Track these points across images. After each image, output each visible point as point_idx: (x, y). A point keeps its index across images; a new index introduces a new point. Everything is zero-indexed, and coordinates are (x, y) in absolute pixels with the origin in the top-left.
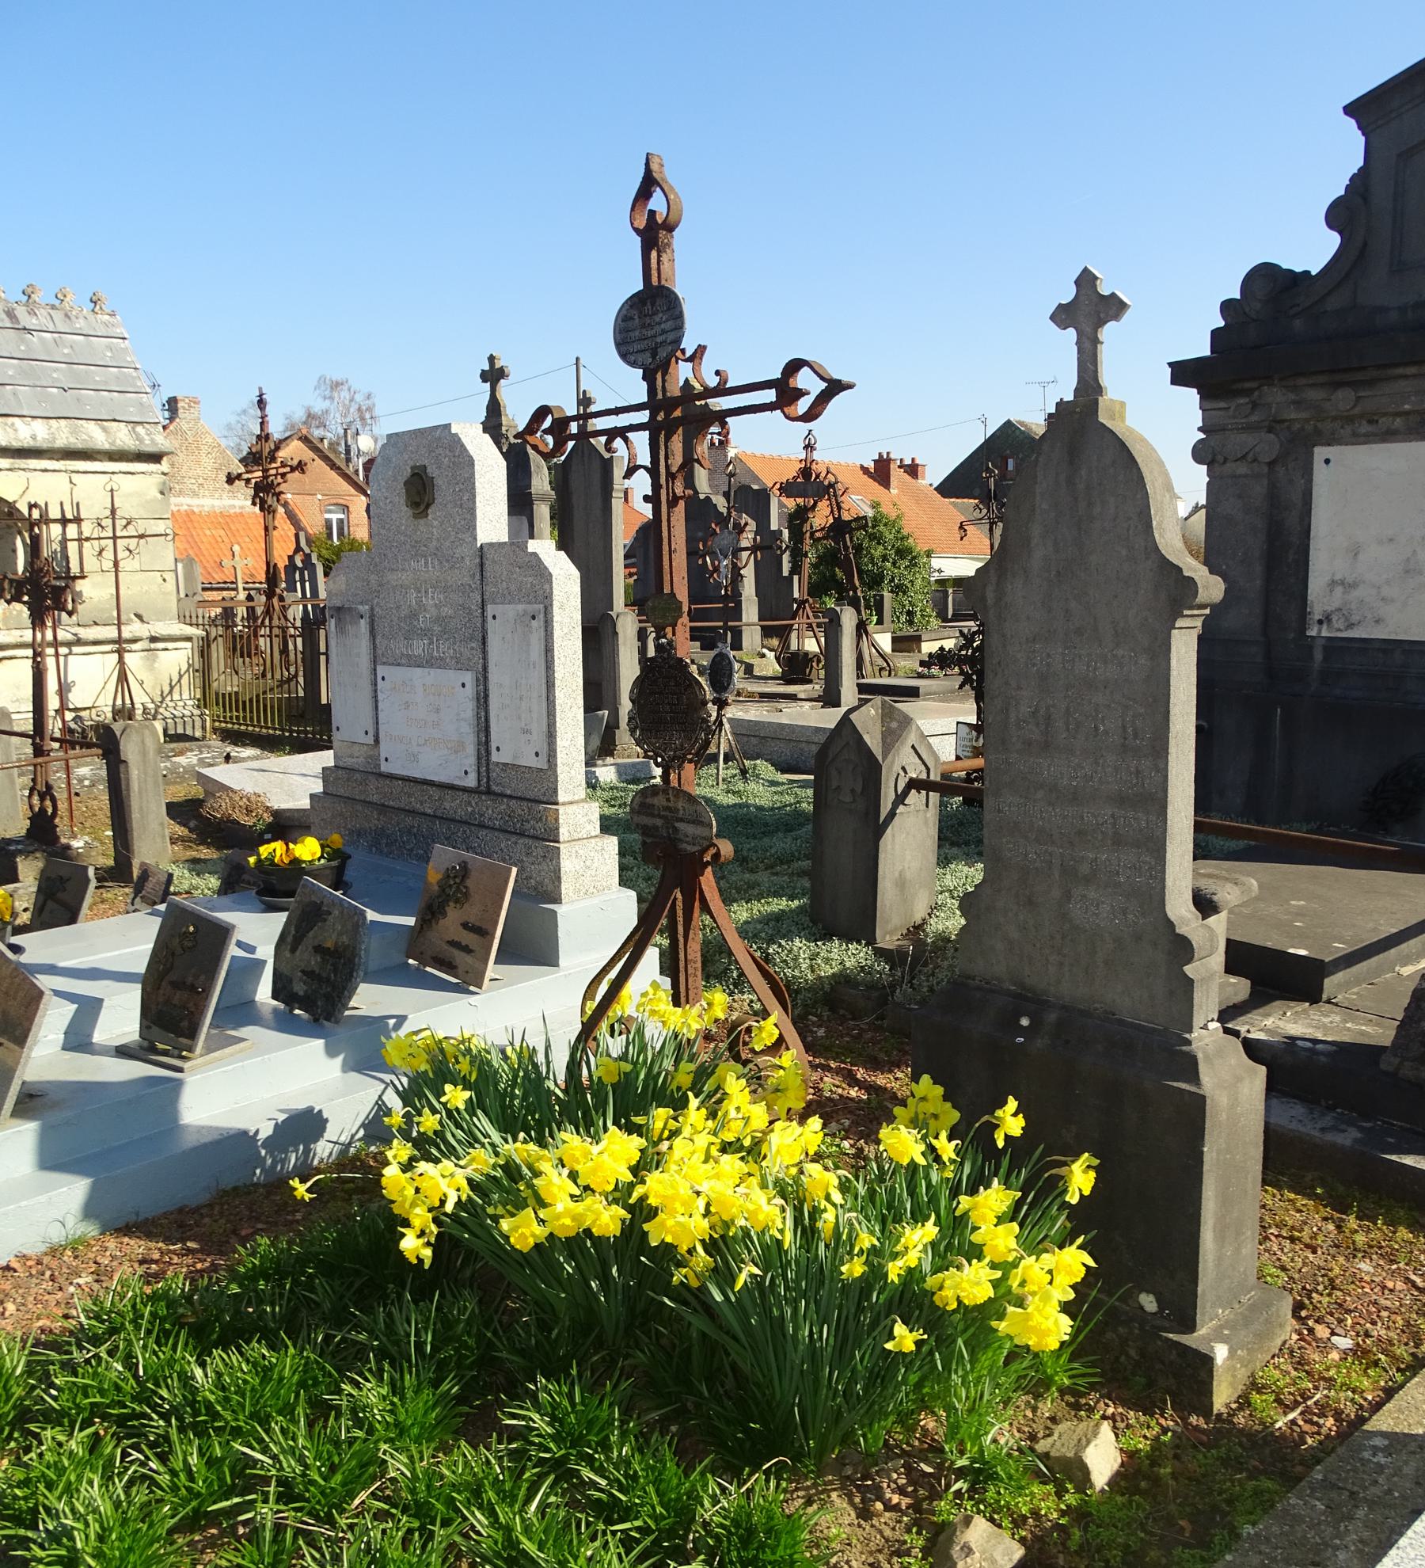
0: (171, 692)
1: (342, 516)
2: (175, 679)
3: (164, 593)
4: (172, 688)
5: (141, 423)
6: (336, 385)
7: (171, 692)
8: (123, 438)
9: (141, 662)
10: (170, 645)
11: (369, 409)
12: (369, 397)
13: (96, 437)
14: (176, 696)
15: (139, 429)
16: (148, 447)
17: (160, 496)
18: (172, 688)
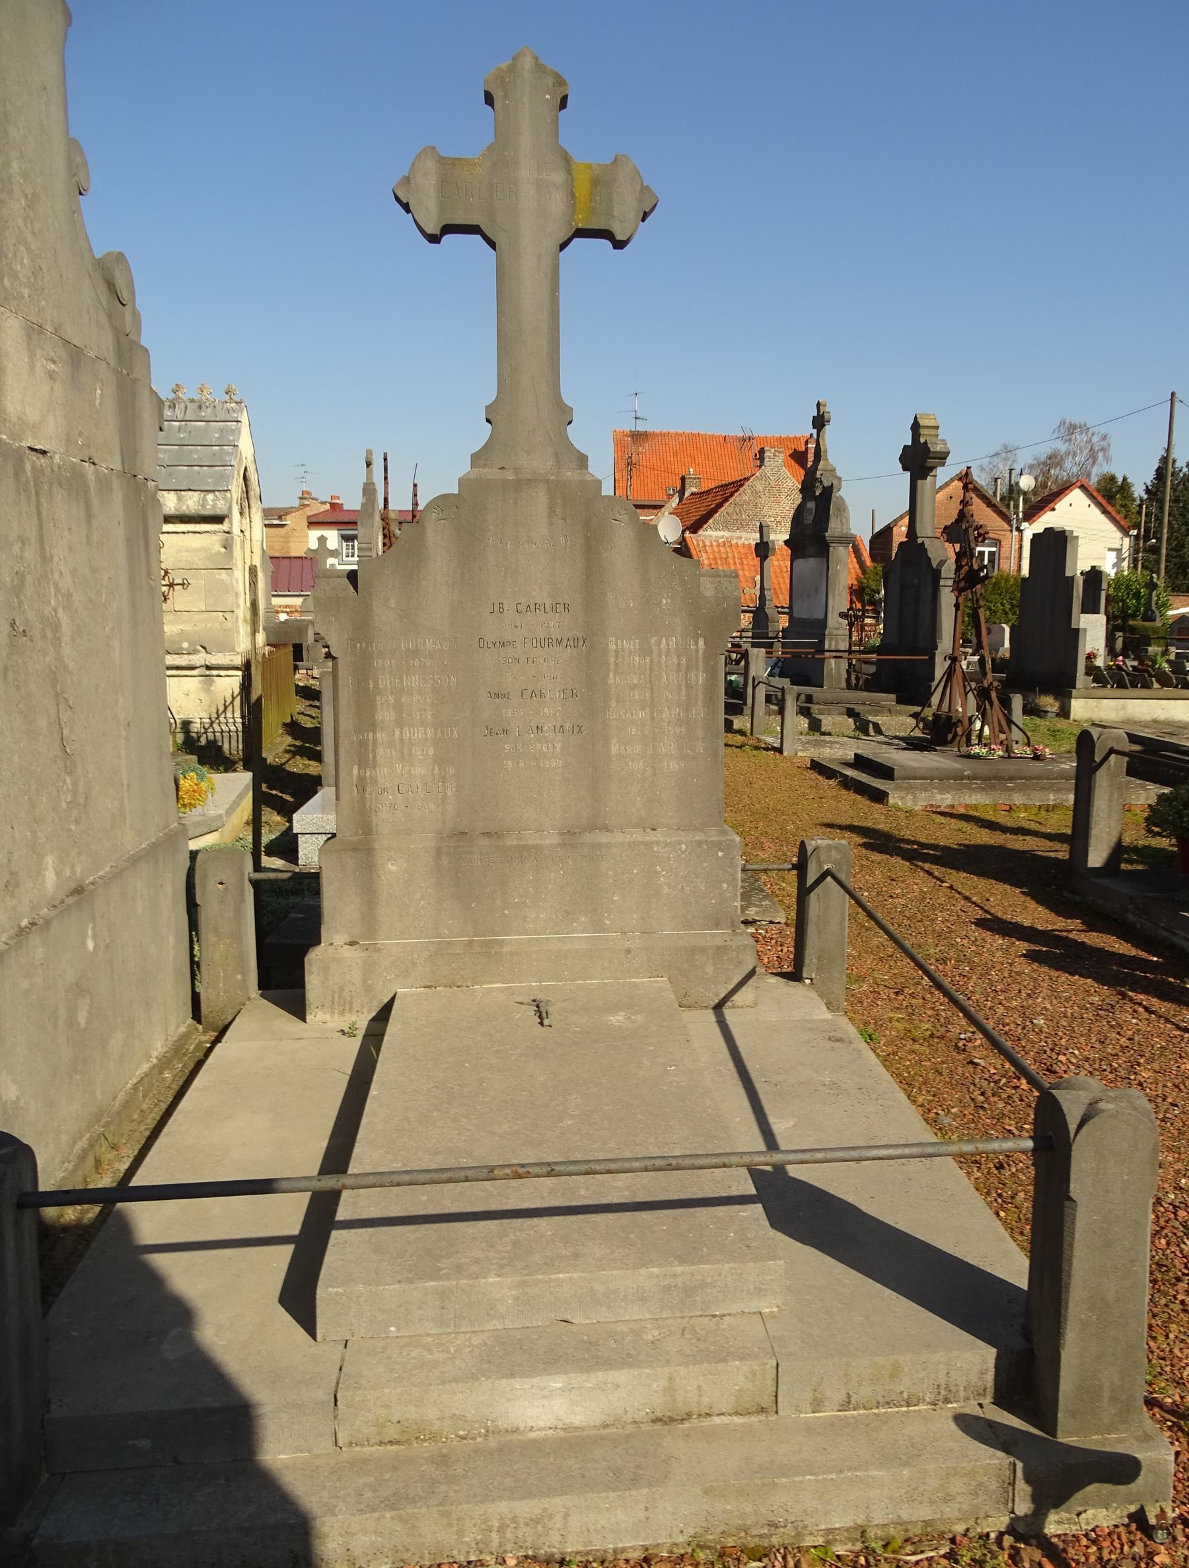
0: (225, 711)
1: (994, 549)
2: (229, 700)
4: (226, 708)
5: (213, 491)
6: (1072, 428)
7: (225, 711)
8: (192, 503)
9: (199, 686)
10: (222, 673)
11: (1103, 449)
12: (1105, 437)
14: (229, 715)
15: (210, 497)
16: (208, 511)
17: (223, 550)
18: (226, 708)
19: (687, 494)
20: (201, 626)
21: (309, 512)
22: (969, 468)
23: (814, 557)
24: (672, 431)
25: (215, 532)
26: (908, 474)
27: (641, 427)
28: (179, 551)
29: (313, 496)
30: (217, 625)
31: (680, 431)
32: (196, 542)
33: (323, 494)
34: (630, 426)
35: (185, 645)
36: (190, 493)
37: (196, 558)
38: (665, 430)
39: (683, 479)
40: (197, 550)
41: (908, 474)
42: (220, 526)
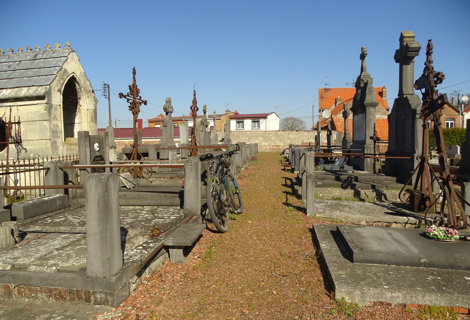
3: (47, 148)
8: (32, 92)
13: (24, 92)
15: (41, 88)
16: (37, 94)
19: (337, 104)
20: (37, 147)
21: (228, 115)
22: (430, 40)
23: (361, 113)
24: (337, 88)
25: (42, 104)
26: (399, 64)
27: (327, 87)
28: (28, 113)
29: (192, 104)
30: (44, 146)
31: (340, 87)
32: (34, 108)
33: (233, 110)
34: (324, 87)
35: (32, 155)
36: (34, 87)
38: (335, 88)
39: (336, 100)
40: (35, 112)
41: (399, 64)
42: (43, 101)
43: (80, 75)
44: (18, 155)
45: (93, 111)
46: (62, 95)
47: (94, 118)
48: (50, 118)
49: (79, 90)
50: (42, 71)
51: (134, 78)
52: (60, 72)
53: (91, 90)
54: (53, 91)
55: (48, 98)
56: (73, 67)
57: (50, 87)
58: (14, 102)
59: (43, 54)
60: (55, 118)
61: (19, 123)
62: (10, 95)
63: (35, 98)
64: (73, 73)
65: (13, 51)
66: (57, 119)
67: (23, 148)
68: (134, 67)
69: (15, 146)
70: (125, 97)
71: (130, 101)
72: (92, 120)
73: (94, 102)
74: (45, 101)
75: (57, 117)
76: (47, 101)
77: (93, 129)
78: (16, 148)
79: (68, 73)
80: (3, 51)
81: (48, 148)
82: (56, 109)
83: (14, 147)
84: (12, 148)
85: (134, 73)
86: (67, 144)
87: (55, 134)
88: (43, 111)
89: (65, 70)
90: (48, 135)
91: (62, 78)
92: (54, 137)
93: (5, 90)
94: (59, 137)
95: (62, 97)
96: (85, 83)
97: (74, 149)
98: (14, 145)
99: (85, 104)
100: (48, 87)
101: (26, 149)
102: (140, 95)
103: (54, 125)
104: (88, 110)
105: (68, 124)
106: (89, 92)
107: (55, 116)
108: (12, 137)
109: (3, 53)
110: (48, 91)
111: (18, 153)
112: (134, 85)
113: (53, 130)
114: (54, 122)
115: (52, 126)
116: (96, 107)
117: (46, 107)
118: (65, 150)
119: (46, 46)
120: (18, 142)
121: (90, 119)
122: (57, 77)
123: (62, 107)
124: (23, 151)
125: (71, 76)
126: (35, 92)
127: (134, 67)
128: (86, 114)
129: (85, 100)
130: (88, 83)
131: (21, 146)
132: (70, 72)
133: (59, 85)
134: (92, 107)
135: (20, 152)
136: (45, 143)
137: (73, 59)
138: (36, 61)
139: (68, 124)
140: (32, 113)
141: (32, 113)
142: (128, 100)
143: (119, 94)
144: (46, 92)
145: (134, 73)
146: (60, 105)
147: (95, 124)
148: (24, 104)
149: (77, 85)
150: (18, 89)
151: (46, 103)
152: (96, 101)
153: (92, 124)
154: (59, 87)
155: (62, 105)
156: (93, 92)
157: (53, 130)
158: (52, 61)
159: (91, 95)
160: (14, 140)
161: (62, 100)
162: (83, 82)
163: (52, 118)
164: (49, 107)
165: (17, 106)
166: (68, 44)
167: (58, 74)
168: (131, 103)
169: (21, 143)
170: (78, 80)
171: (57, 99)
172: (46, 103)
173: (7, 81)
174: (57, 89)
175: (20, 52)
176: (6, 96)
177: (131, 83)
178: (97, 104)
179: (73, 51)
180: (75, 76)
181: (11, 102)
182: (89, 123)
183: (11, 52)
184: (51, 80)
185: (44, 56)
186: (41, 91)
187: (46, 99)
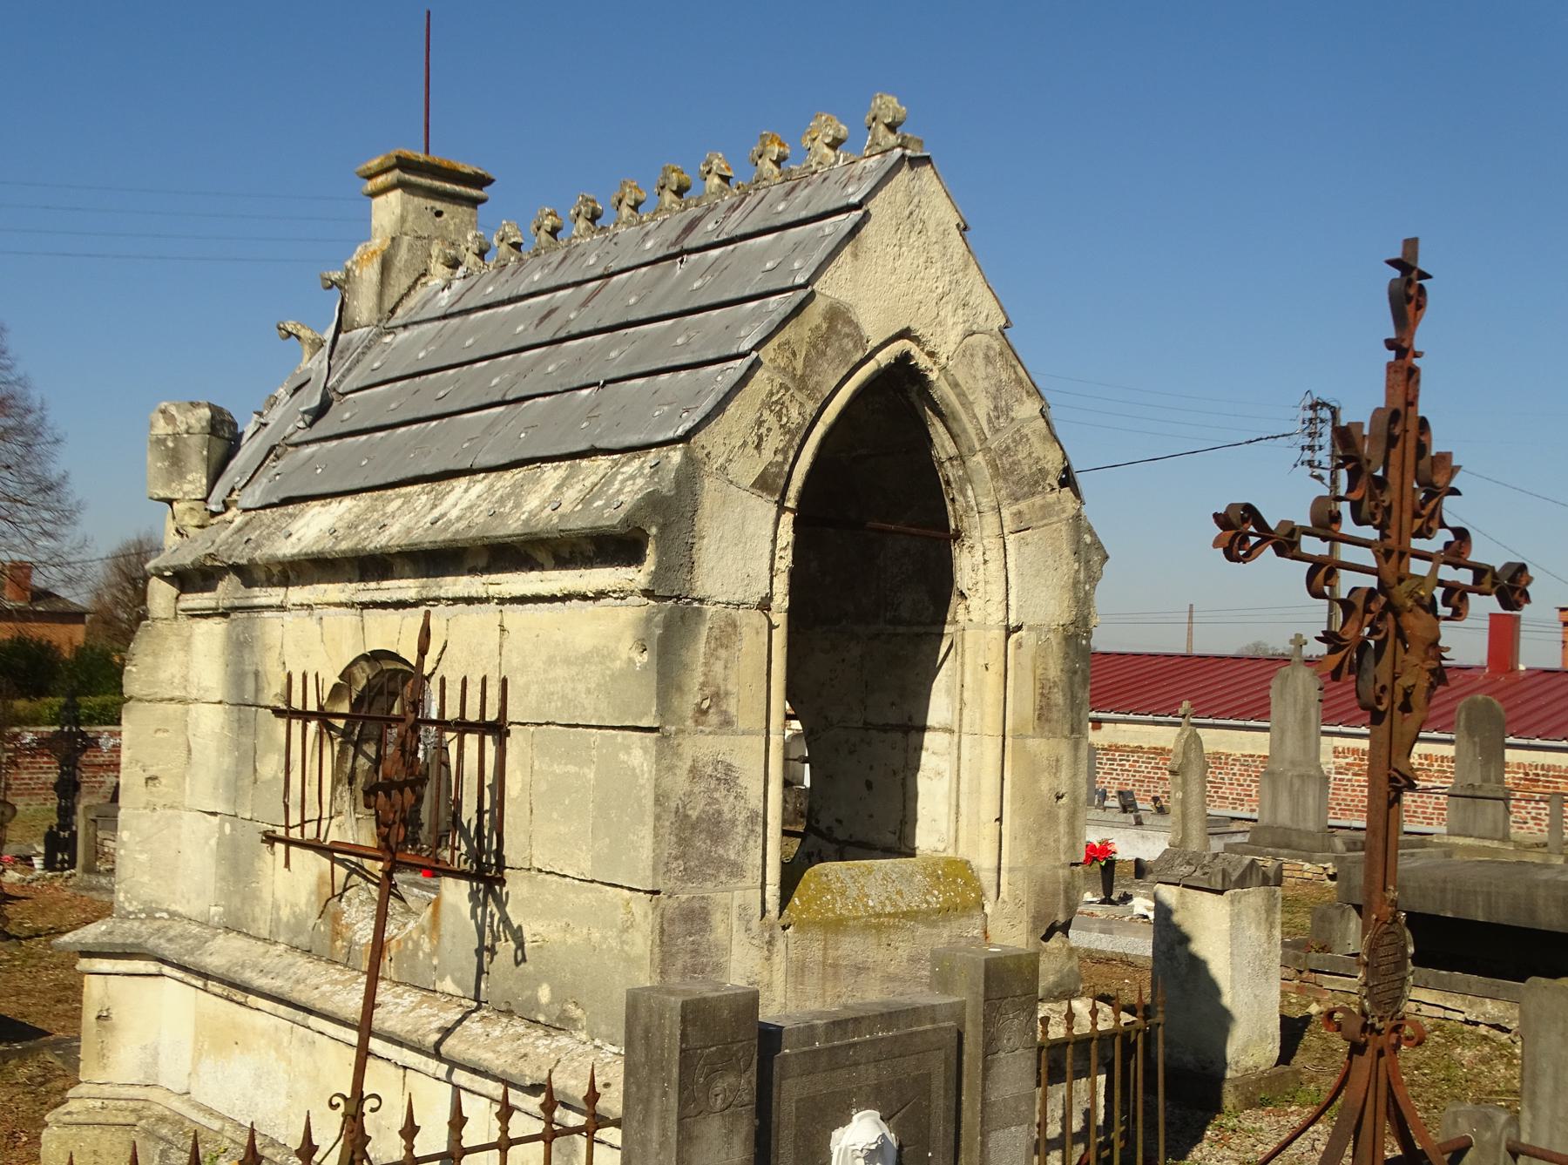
25: (623, 594)
35: (544, 994)
37: (581, 687)
40: (585, 659)
43: (966, 353)
44: (480, 971)
45: (1055, 640)
46: (787, 519)
47: (1058, 698)
48: (664, 707)
49: (951, 472)
50: (687, 339)
51: (1401, 348)
52: (788, 333)
53: (1053, 461)
54: (710, 488)
55: (662, 552)
56: (911, 282)
57: (689, 459)
58: (488, 570)
59: (733, 208)
60: (713, 709)
61: (498, 730)
62: (461, 525)
63: (590, 549)
64: (905, 334)
65: (594, 217)
66: (727, 722)
67: (505, 920)
68: (1411, 245)
69: (473, 896)
70: (1286, 544)
71: (1346, 582)
72: (1043, 714)
73: (1068, 567)
74: (636, 577)
75: (731, 706)
76: (656, 576)
77: (1045, 785)
78: (474, 915)
79: (860, 341)
80: (548, 223)
81: (630, 961)
82: (728, 633)
83: (466, 907)
84: (456, 909)
85: (1408, 293)
86: (802, 927)
87: (701, 843)
88: (631, 656)
89: (837, 315)
90: (641, 850)
91: (802, 382)
92: (688, 875)
93: (463, 482)
94: (736, 870)
95: (786, 535)
96: (1000, 411)
97: (860, 969)
98: (464, 886)
99: (1001, 586)
100: (676, 456)
101: (517, 936)
102: (1453, 511)
103: (694, 772)
104: (1009, 631)
105: (885, 728)
106: (1034, 483)
107: (717, 697)
108: (465, 833)
109: (554, 232)
110: (667, 488)
111: (479, 953)
112: (1402, 423)
113: (682, 817)
114: (701, 746)
115: (680, 782)
116: (1083, 604)
117: (648, 620)
118: (779, 977)
119: (757, 149)
120: (488, 876)
121: (1023, 702)
122: (761, 375)
123: (780, 619)
124: (506, 948)
125: (884, 358)
126: (586, 500)
127: (1411, 245)
128: (996, 667)
129: (994, 555)
130: (1028, 409)
131: (501, 904)
132: (874, 327)
133: (775, 441)
134: (1046, 605)
135: (492, 951)
136: (621, 915)
137: (911, 220)
138: (679, 269)
139: (885, 728)
140: (567, 661)
141: (567, 661)
142: (1321, 575)
143: (1222, 520)
144: (653, 503)
145: (1408, 293)
146: (765, 605)
147: (1063, 748)
148: (545, 589)
149: (938, 431)
150: (518, 474)
151: (647, 593)
152: (1088, 553)
153: (1039, 746)
154: (768, 454)
155: (781, 601)
156: (1067, 480)
157: (682, 817)
158: (765, 253)
159: (1046, 510)
160: (476, 854)
161: (785, 562)
162: (983, 408)
163: (688, 709)
164: (675, 619)
165: (502, 601)
166: (888, 105)
167: (767, 354)
168: (1347, 606)
169: (502, 882)
170: (942, 389)
171: (746, 552)
172: (647, 593)
173: (495, 422)
174: (749, 468)
175: (626, 211)
176: (450, 523)
177: (1362, 403)
178: (1093, 579)
179: (916, 162)
180: (922, 361)
181: (473, 571)
182: (1019, 736)
183: (582, 224)
184: (707, 405)
185: (731, 227)
186: (617, 489)
187: (650, 564)
